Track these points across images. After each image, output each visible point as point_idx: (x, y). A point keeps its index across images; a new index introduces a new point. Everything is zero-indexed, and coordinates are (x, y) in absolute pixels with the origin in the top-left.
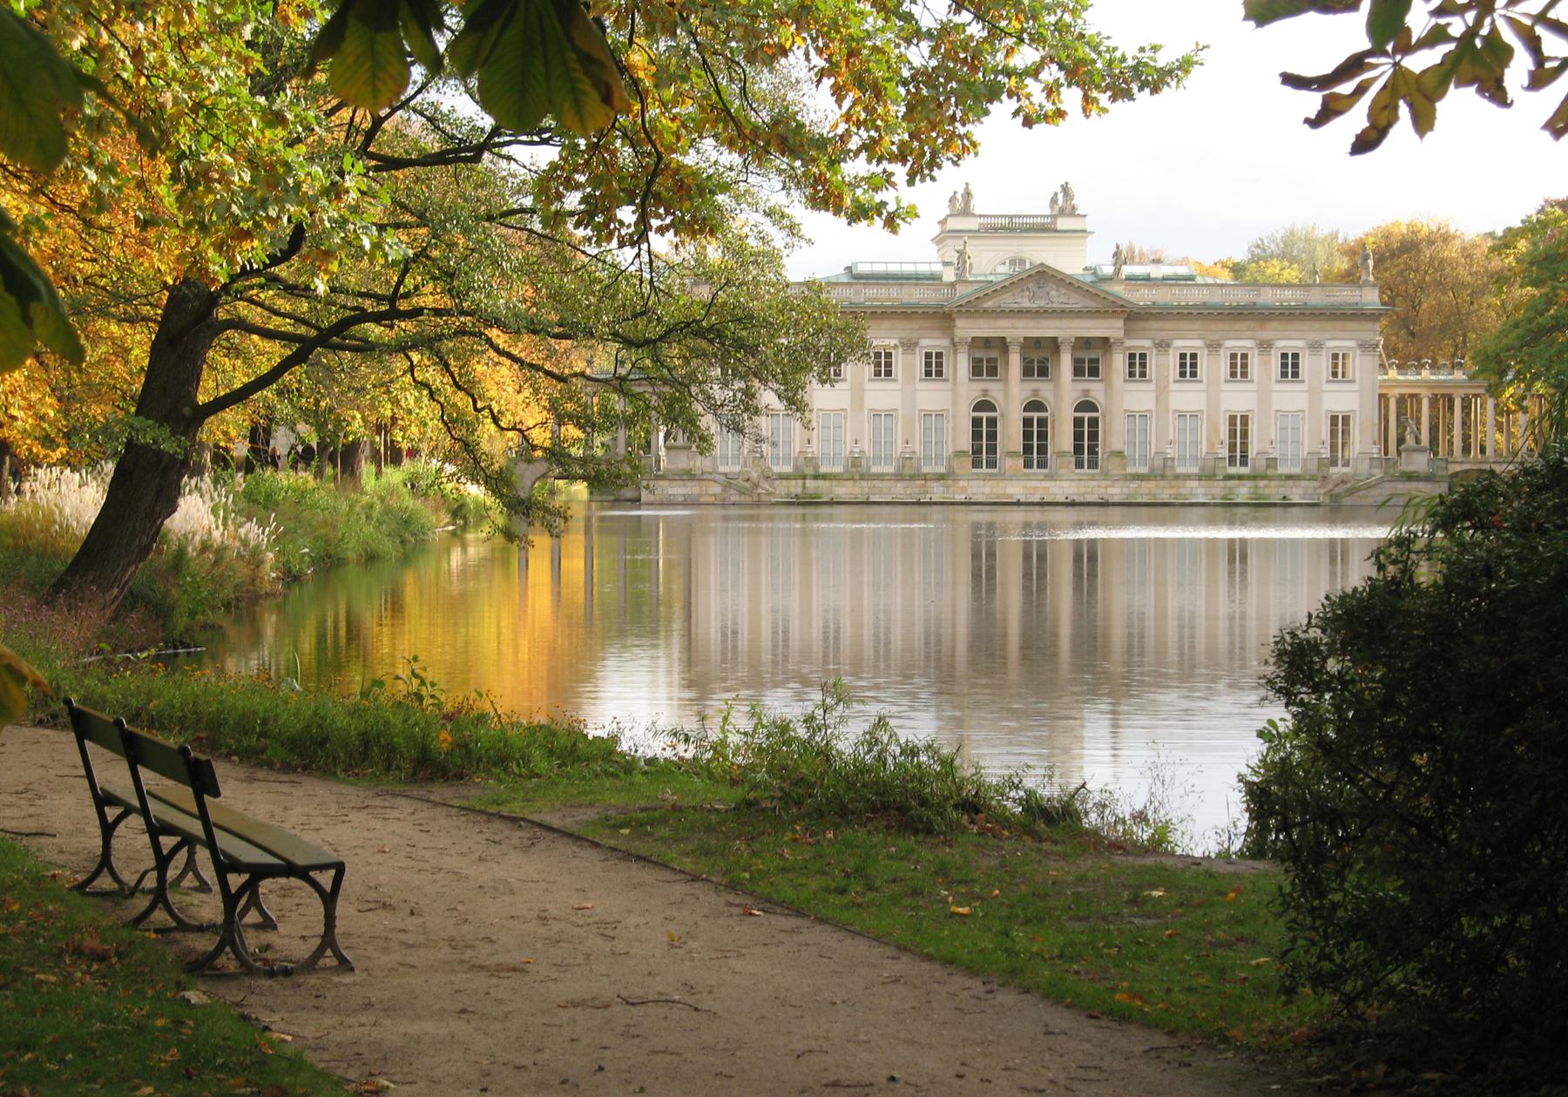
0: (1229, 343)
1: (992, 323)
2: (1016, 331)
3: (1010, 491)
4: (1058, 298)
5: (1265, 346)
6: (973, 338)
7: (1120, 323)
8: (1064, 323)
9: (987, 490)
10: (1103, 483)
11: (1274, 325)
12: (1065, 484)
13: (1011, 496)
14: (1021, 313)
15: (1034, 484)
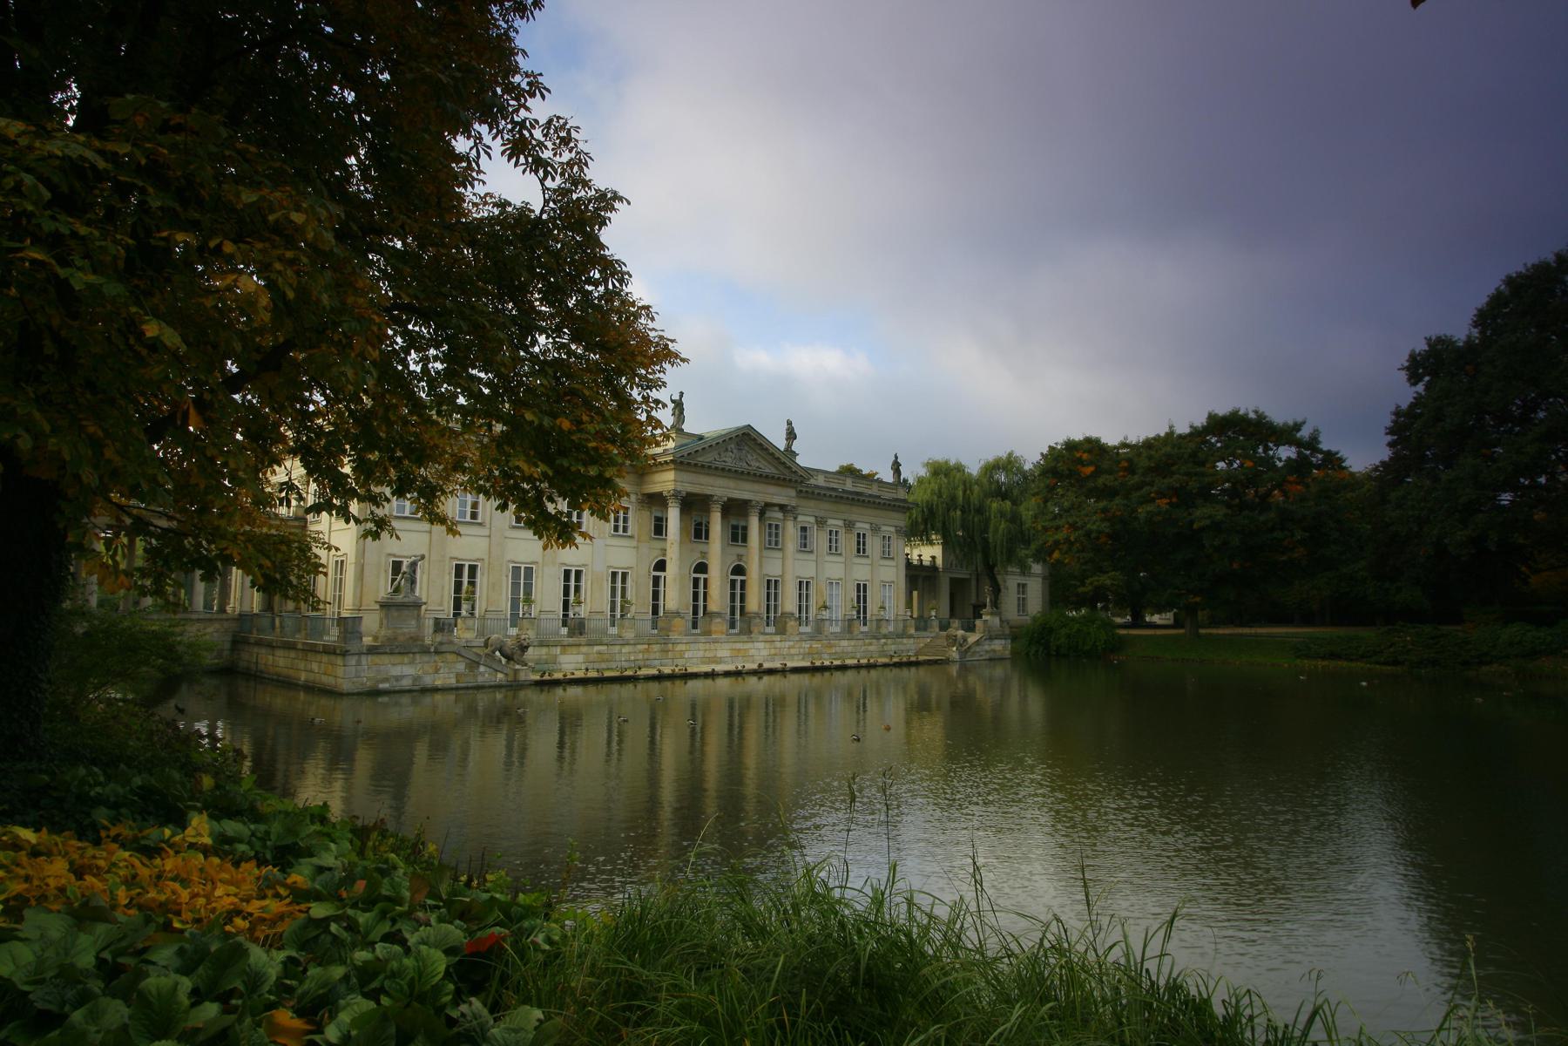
0: (830, 522)
1: (704, 479)
2: (722, 489)
3: (720, 654)
4: (757, 463)
5: (849, 525)
6: (689, 494)
7: (793, 493)
8: (757, 487)
9: (701, 654)
10: (787, 644)
11: (854, 509)
12: (761, 645)
13: (719, 661)
14: (724, 472)
15: (739, 646)
